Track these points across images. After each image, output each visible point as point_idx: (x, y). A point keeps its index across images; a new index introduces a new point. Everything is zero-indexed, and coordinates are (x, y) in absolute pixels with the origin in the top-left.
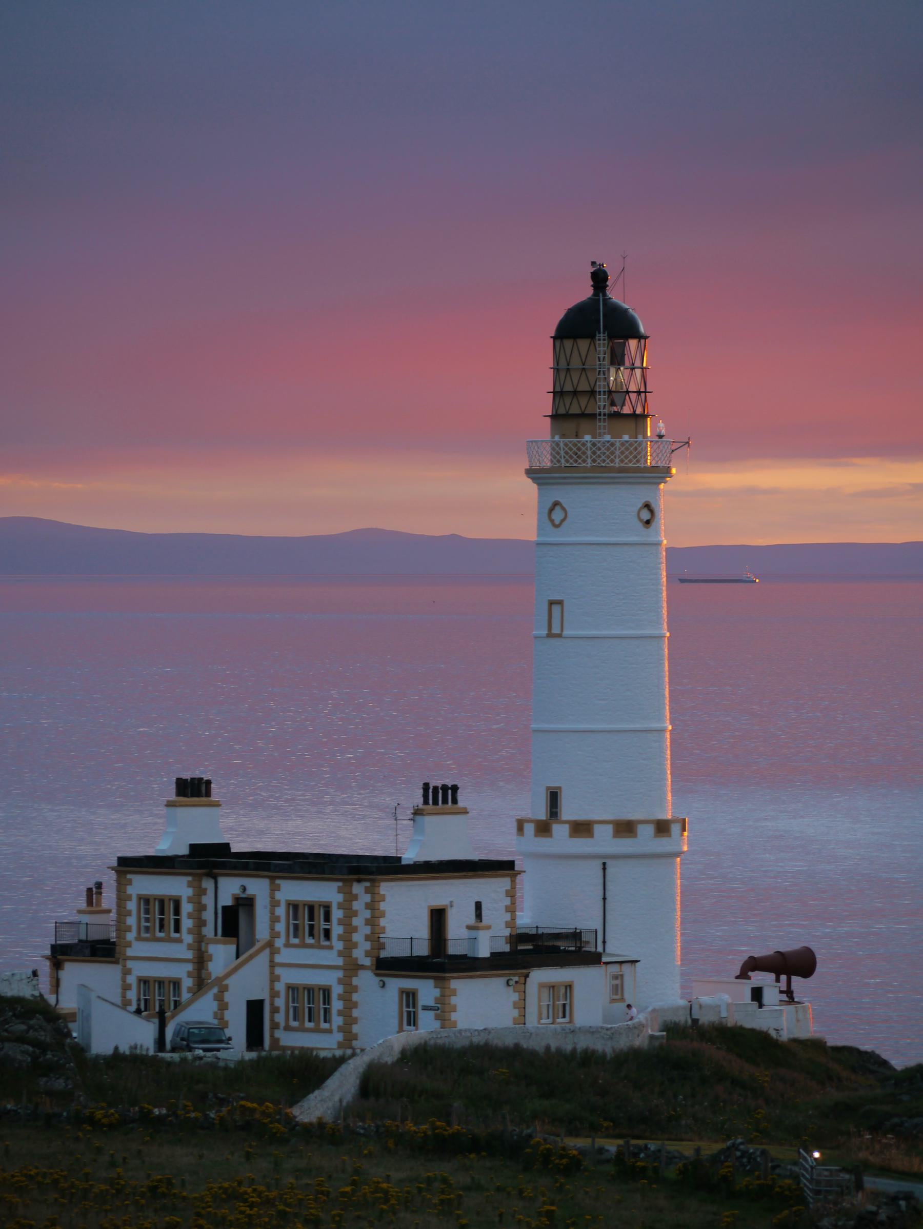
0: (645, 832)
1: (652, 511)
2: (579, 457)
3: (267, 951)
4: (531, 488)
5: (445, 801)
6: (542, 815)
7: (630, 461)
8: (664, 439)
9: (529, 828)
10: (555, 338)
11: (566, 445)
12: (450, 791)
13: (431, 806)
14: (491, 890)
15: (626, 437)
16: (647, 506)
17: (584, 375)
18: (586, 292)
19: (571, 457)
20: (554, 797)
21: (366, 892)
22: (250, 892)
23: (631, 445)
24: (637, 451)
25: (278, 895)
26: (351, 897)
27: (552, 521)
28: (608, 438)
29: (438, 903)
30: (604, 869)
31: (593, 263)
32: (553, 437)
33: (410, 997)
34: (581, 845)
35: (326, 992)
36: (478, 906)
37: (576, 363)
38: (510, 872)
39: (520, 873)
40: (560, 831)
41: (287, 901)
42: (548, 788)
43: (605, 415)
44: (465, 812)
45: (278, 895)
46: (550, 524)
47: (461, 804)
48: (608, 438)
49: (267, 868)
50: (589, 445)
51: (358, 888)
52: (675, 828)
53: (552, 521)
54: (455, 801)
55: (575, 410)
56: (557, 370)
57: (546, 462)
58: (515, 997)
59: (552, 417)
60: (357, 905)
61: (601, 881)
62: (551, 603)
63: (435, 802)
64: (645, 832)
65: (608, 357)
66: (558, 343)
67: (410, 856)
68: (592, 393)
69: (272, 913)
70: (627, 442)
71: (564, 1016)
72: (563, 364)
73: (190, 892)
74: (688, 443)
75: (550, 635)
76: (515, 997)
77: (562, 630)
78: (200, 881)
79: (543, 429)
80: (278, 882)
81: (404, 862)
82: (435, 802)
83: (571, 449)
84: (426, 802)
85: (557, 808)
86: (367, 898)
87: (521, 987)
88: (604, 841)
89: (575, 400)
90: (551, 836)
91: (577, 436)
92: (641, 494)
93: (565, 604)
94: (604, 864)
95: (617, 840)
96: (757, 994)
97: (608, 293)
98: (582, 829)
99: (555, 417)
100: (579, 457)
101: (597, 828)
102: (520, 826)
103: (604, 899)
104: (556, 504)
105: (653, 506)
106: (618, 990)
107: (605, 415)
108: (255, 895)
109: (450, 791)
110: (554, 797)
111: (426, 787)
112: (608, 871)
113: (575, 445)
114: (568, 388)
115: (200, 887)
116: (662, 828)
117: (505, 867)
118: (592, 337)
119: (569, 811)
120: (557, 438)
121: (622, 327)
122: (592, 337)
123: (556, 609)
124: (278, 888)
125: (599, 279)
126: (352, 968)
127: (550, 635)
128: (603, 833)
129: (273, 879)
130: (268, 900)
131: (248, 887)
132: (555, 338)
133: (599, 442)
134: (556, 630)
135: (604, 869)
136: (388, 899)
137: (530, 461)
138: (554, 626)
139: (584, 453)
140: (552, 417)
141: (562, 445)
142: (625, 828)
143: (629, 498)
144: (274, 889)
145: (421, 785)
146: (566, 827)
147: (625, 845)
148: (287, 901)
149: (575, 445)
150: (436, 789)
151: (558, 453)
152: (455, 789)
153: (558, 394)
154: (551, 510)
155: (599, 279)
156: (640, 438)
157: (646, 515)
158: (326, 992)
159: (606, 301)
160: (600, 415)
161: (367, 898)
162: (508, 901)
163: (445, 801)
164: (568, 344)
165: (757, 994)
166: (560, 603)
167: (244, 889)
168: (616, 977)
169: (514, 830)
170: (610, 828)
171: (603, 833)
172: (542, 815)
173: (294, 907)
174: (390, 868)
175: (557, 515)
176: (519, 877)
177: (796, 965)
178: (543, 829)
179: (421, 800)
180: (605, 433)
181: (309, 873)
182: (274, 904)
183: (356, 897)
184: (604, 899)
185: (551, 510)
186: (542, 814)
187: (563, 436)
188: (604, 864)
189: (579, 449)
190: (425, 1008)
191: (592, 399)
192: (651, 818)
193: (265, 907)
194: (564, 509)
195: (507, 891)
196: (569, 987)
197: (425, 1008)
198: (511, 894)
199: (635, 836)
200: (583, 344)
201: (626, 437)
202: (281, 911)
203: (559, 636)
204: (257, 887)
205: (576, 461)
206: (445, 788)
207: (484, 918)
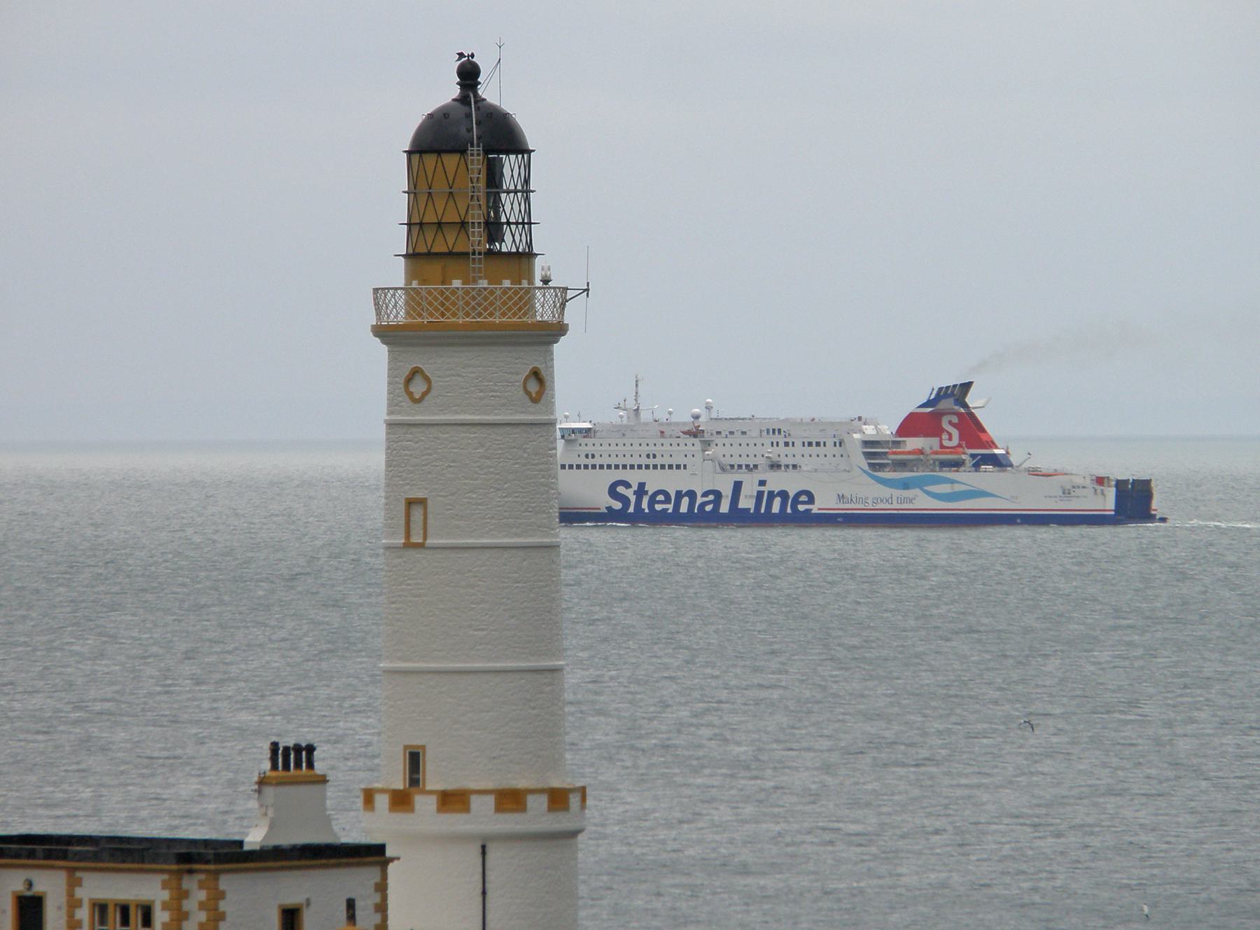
0: (537, 804)
2: (448, 309)
4: (381, 351)
5: (298, 765)
6: (399, 783)
7: (514, 315)
8: (551, 284)
9: (382, 801)
10: (409, 153)
11: (430, 293)
12: (304, 753)
13: (280, 773)
14: (357, 882)
15: (507, 283)
16: (536, 374)
17: (451, 201)
18: (451, 90)
19: (436, 309)
20: (415, 760)
21: (201, 887)
22: (38, 888)
23: (492, 293)
24: (524, 300)
25: (80, 893)
26: (184, 894)
27: (410, 394)
28: (483, 283)
29: (291, 900)
30: (484, 853)
31: (461, 55)
32: (408, 282)
34: (455, 822)
36: (351, 904)
37: (440, 186)
38: (381, 859)
39: (392, 860)
40: (425, 804)
41: (91, 900)
42: (406, 747)
43: (480, 254)
44: (323, 780)
45: (80, 893)
46: (406, 397)
47: (319, 767)
48: (483, 283)
49: (64, 856)
50: (460, 292)
51: (190, 883)
52: (574, 800)
53: (410, 394)
54: (310, 765)
55: (440, 247)
56: (413, 192)
57: (398, 314)
59: (406, 256)
60: (190, 905)
61: (480, 870)
62: (410, 503)
63: (286, 766)
64: (537, 804)
65: (483, 176)
66: (416, 158)
67: (255, 838)
68: (463, 224)
69: (71, 916)
70: (485, 289)
72: (423, 187)
73: (165, 895)
74: (587, 290)
75: (408, 545)
77: (425, 538)
78: (180, 880)
79: (395, 274)
80: (78, 874)
81: (246, 848)
82: (286, 766)
83: (436, 299)
84: (274, 767)
85: (418, 772)
86: (202, 895)
88: (483, 817)
89: (463, 234)
90: (412, 810)
91: (443, 283)
92: (526, 360)
93: (429, 502)
94: (484, 847)
95: (394, 815)
97: (480, 92)
98: (453, 800)
99: (412, 256)
100: (448, 309)
101: (475, 801)
102: (369, 797)
103: (484, 893)
104: (416, 372)
105: (543, 373)
107: (480, 254)
108: (45, 893)
109: (304, 753)
110: (415, 760)
111: (275, 746)
112: (489, 856)
113: (442, 293)
114: (430, 218)
115: (179, 888)
116: (558, 799)
117: (373, 854)
118: (463, 151)
119: (435, 779)
120: (415, 284)
121: (502, 136)
122: (463, 151)
123: (417, 514)
124: (79, 883)
125: (469, 74)
127: (408, 545)
128: (483, 806)
129: (71, 871)
130: (63, 899)
131: (36, 881)
132: (409, 153)
133: (473, 289)
134: (417, 539)
135: (484, 853)
136: (229, 896)
137: (378, 313)
138: (413, 532)
139: (454, 304)
140: (406, 256)
141: (424, 293)
142: (510, 800)
143: (511, 365)
144: (73, 883)
145: (266, 747)
147: (510, 823)
148: (91, 900)
149: (442, 293)
150: (286, 749)
151: (419, 304)
152: (310, 749)
153: (415, 226)
154: (409, 380)
155: (469, 74)
156: (525, 284)
157: (533, 387)
159: (479, 100)
160: (474, 254)
161: (202, 895)
162: (377, 898)
163: (298, 765)
164: (430, 159)
166: (422, 502)
167: (30, 884)
169: (360, 802)
170: (490, 800)
171: (483, 806)
172: (399, 783)
173: (101, 909)
174: (229, 855)
175: (418, 387)
176: (391, 867)
178: (401, 801)
179: (267, 765)
180: (481, 278)
181: (123, 862)
182: (74, 904)
183: (186, 894)
184: (484, 893)
185: (409, 380)
186: (399, 782)
187: (423, 282)
188: (484, 847)
189: (447, 299)
191: (463, 234)
192: (540, 786)
193: (59, 908)
194: (427, 380)
195: (376, 884)
198: (382, 888)
199: (412, 810)
200: (451, 161)
201: (457, 283)
202: (83, 914)
203: (420, 546)
204: (49, 883)
205: (443, 315)
206: (298, 749)
207: (358, 917)
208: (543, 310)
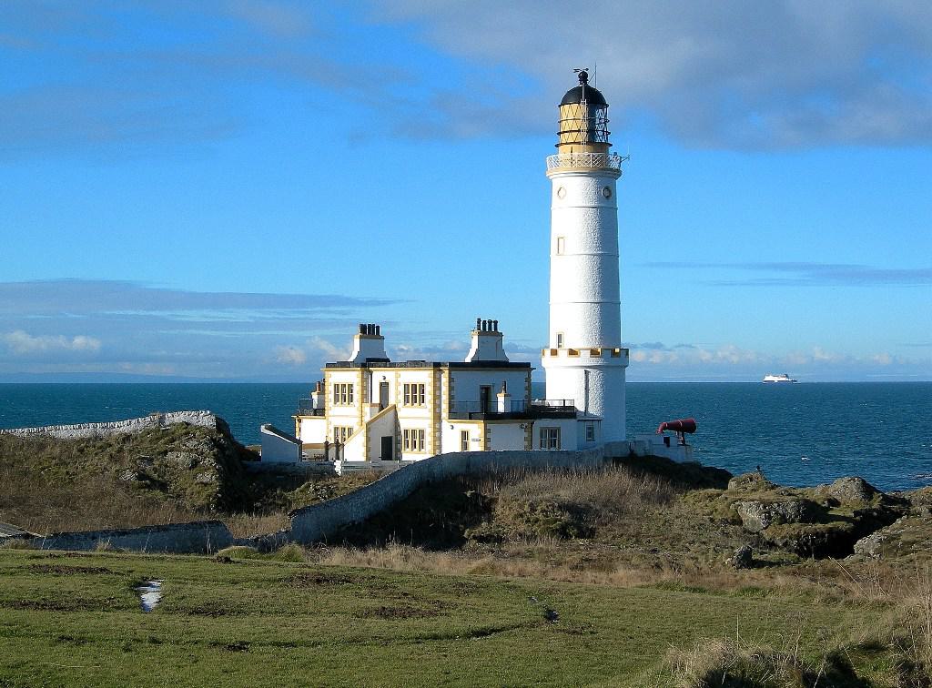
1: (610, 191)
3: (393, 411)
25: (399, 380)
29: (485, 384)
33: (465, 435)
34: (574, 360)
35: (422, 433)
40: (563, 353)
45: (399, 380)
58: (526, 435)
71: (555, 446)
76: (526, 435)
87: (530, 430)
96: (667, 440)
98: (572, 352)
106: (590, 434)
125: (584, 77)
126: (437, 418)
146: (566, 353)
155: (584, 77)
158: (422, 433)
165: (667, 440)
168: (590, 428)
177: (689, 428)
182: (398, 384)
190: (473, 440)
196: (554, 432)
197: (473, 440)
206: (490, 322)
208: (614, 165)
